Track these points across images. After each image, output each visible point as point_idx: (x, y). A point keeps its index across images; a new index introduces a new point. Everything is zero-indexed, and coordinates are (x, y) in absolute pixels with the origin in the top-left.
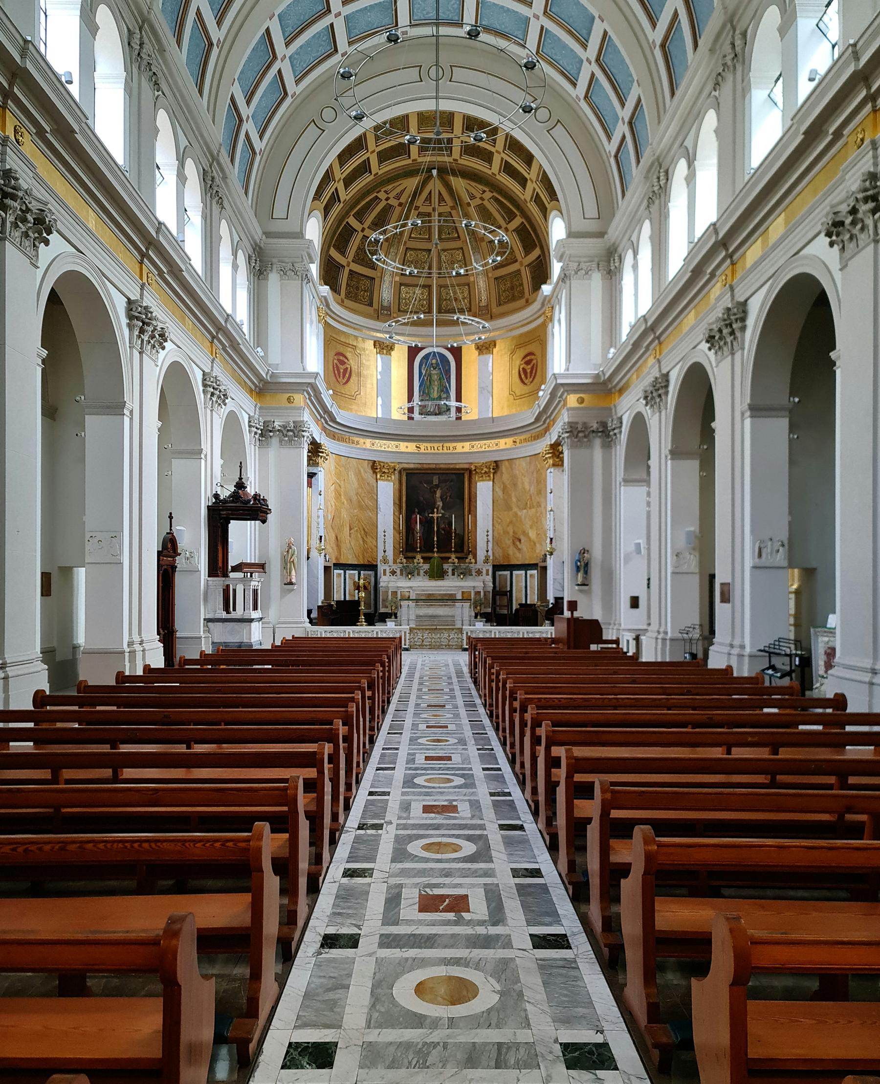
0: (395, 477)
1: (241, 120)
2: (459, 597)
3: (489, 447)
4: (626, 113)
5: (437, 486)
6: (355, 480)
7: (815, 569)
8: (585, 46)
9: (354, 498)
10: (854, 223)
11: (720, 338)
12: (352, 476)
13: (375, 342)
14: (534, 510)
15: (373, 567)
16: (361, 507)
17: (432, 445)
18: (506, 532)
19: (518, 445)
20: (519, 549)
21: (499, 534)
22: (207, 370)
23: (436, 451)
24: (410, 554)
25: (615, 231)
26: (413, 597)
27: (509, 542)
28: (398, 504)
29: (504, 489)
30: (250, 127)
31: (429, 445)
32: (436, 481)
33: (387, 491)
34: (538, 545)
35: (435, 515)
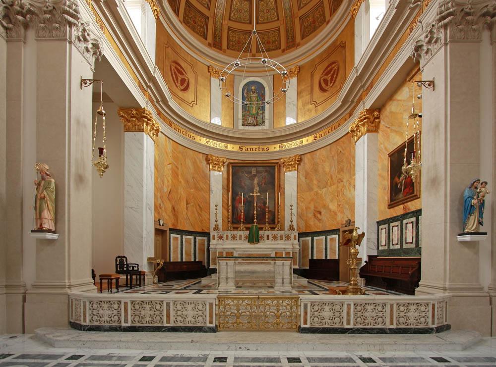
0: (224, 169)
2: (273, 255)
3: (294, 145)
5: (255, 176)
6: (191, 167)
9: (191, 181)
12: (189, 163)
13: (209, 67)
14: (334, 187)
15: (206, 234)
16: (197, 188)
17: (252, 147)
18: (308, 208)
19: (318, 138)
20: (319, 220)
21: (302, 210)
23: (254, 151)
24: (235, 226)
26: (235, 255)
27: (310, 215)
28: (226, 189)
29: (307, 176)
31: (249, 147)
32: (254, 171)
33: (218, 177)
34: (339, 214)
35: (255, 194)
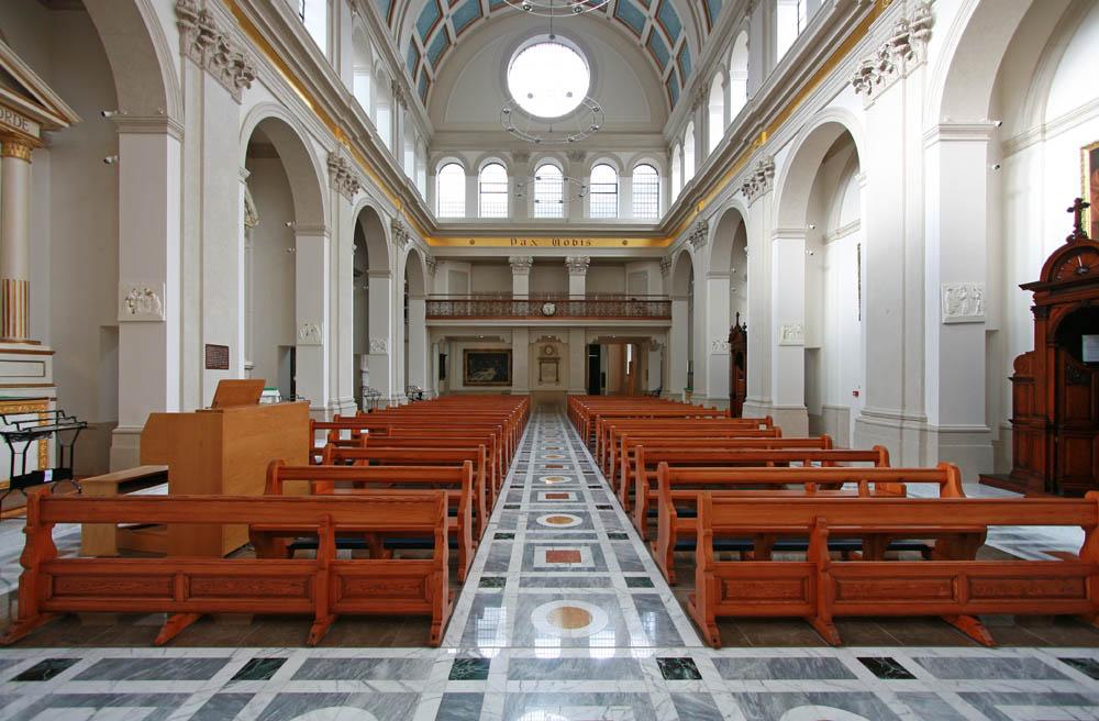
1: (419, 57)
4: (674, 52)
7: (818, 349)
8: (648, 8)
10: (883, 68)
11: (754, 186)
22: (394, 217)
25: (669, 130)
30: (425, 61)
